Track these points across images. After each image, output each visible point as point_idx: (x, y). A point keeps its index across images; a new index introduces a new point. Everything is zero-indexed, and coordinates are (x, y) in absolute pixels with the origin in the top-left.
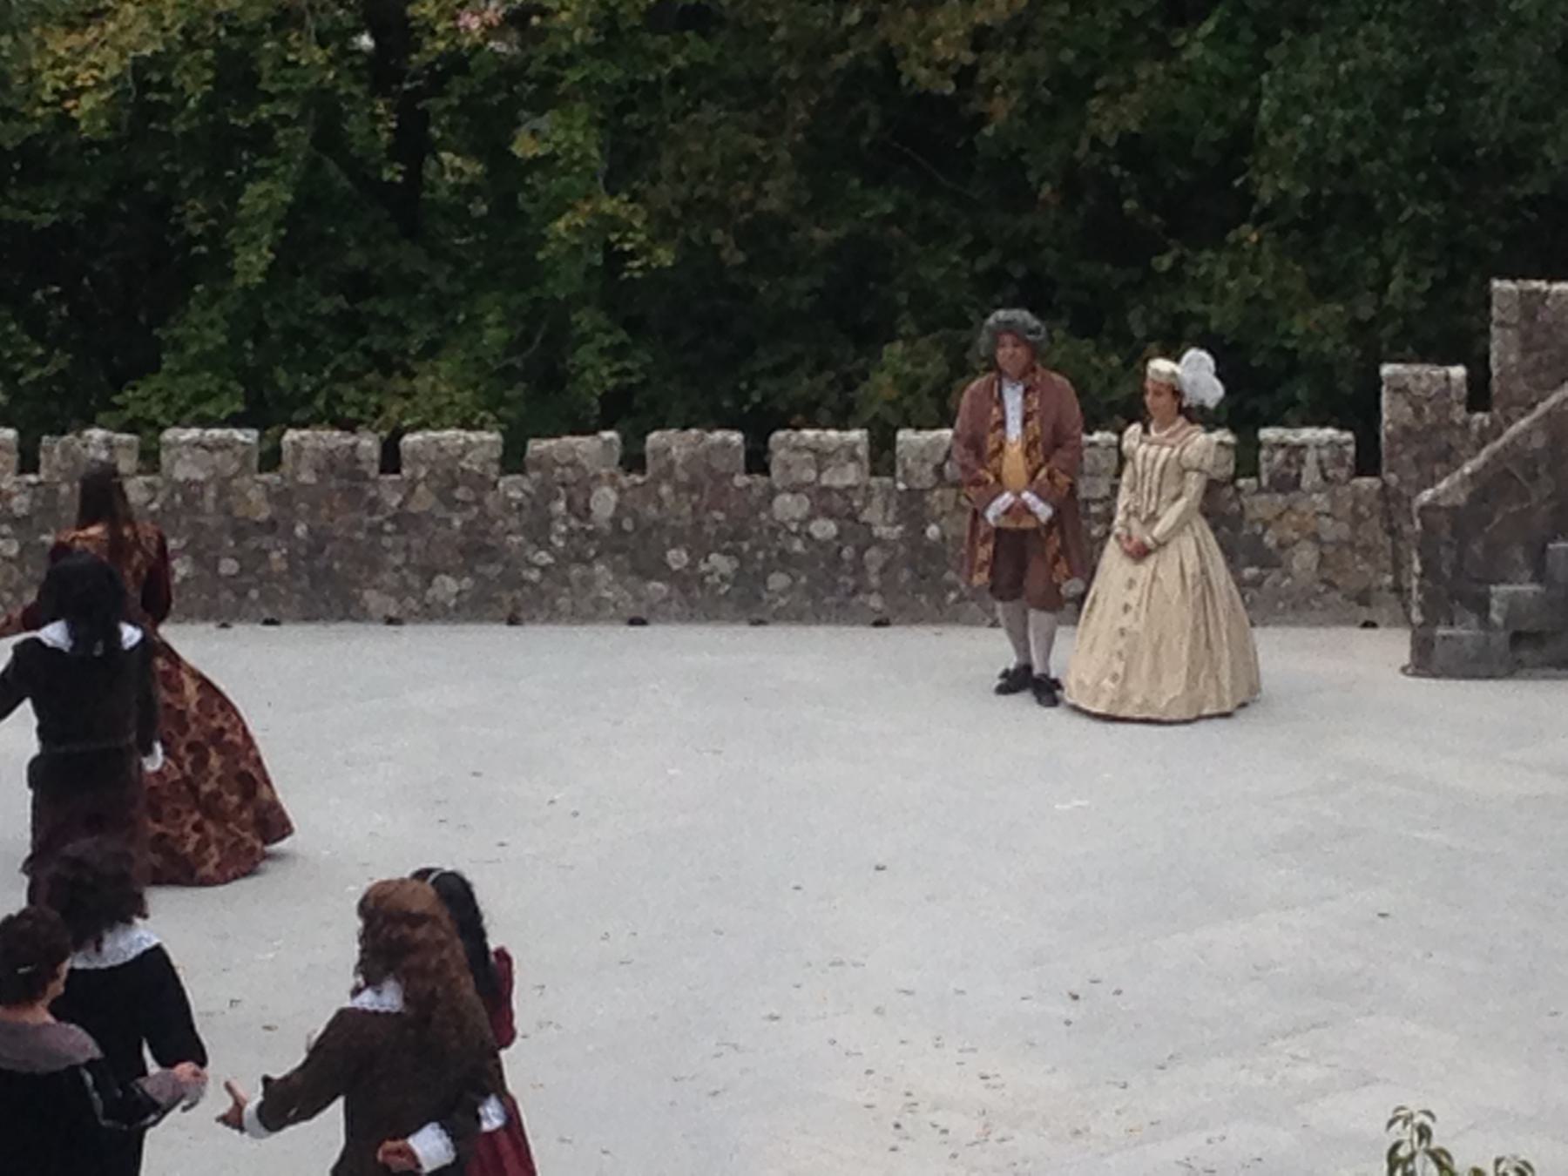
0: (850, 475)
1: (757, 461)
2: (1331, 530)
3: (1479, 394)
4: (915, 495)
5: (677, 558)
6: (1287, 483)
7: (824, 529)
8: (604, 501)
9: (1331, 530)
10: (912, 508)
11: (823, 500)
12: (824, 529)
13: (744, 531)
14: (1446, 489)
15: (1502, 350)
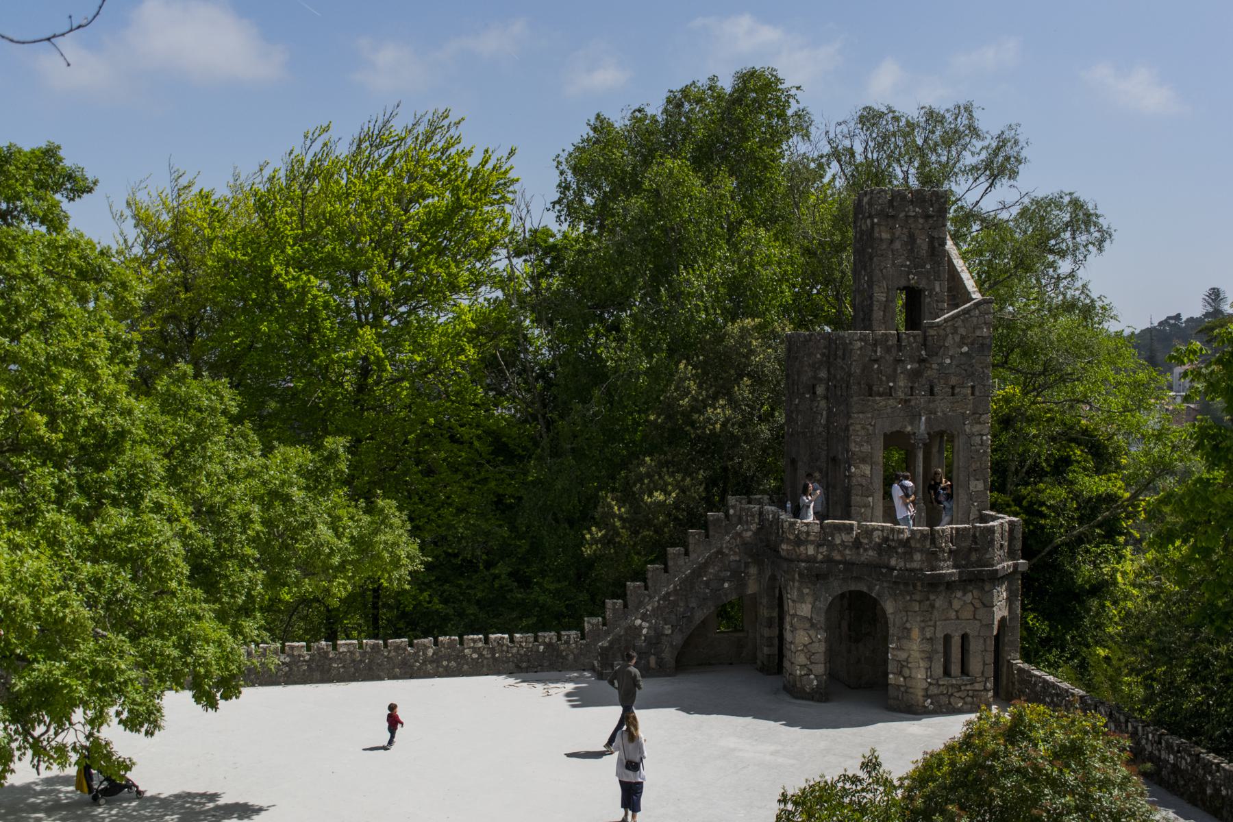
0: (480, 645)
1: (461, 642)
2: (576, 651)
3: (604, 624)
4: (493, 648)
5: (445, 663)
6: (567, 642)
7: (475, 656)
8: (430, 652)
9: (576, 651)
10: (493, 650)
11: (474, 650)
12: (475, 656)
13: (460, 657)
14: (604, 643)
15: (609, 614)
